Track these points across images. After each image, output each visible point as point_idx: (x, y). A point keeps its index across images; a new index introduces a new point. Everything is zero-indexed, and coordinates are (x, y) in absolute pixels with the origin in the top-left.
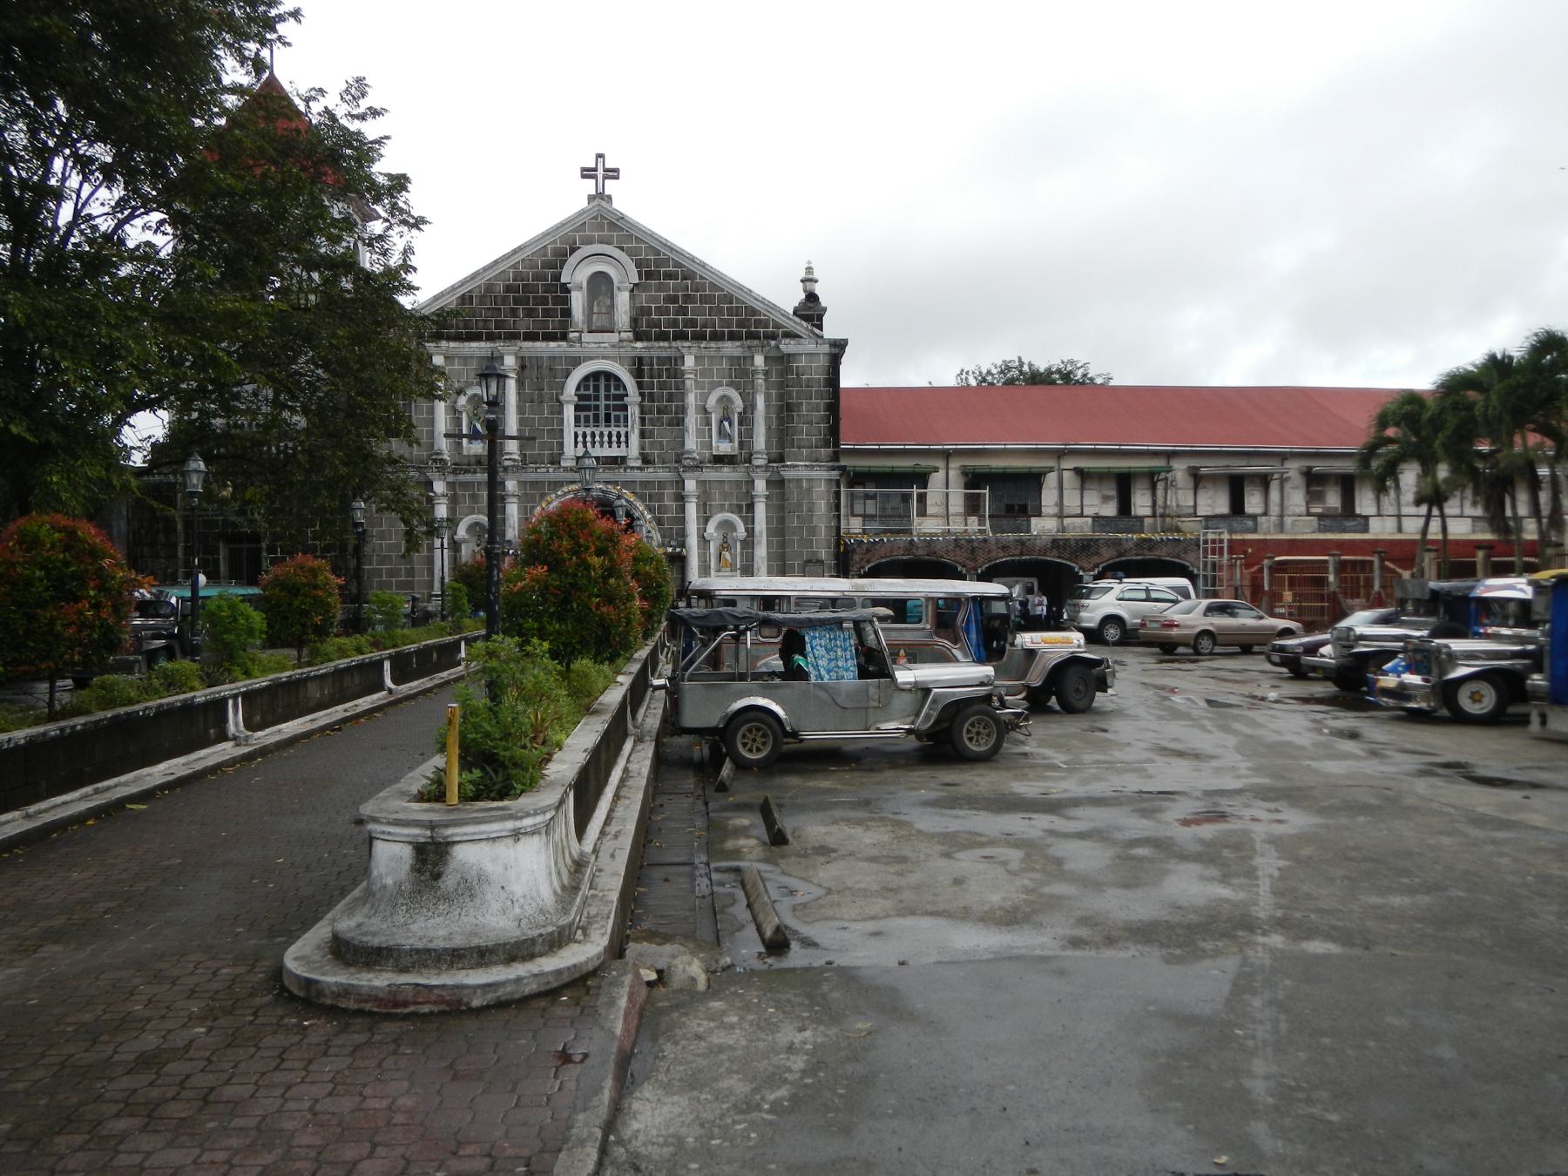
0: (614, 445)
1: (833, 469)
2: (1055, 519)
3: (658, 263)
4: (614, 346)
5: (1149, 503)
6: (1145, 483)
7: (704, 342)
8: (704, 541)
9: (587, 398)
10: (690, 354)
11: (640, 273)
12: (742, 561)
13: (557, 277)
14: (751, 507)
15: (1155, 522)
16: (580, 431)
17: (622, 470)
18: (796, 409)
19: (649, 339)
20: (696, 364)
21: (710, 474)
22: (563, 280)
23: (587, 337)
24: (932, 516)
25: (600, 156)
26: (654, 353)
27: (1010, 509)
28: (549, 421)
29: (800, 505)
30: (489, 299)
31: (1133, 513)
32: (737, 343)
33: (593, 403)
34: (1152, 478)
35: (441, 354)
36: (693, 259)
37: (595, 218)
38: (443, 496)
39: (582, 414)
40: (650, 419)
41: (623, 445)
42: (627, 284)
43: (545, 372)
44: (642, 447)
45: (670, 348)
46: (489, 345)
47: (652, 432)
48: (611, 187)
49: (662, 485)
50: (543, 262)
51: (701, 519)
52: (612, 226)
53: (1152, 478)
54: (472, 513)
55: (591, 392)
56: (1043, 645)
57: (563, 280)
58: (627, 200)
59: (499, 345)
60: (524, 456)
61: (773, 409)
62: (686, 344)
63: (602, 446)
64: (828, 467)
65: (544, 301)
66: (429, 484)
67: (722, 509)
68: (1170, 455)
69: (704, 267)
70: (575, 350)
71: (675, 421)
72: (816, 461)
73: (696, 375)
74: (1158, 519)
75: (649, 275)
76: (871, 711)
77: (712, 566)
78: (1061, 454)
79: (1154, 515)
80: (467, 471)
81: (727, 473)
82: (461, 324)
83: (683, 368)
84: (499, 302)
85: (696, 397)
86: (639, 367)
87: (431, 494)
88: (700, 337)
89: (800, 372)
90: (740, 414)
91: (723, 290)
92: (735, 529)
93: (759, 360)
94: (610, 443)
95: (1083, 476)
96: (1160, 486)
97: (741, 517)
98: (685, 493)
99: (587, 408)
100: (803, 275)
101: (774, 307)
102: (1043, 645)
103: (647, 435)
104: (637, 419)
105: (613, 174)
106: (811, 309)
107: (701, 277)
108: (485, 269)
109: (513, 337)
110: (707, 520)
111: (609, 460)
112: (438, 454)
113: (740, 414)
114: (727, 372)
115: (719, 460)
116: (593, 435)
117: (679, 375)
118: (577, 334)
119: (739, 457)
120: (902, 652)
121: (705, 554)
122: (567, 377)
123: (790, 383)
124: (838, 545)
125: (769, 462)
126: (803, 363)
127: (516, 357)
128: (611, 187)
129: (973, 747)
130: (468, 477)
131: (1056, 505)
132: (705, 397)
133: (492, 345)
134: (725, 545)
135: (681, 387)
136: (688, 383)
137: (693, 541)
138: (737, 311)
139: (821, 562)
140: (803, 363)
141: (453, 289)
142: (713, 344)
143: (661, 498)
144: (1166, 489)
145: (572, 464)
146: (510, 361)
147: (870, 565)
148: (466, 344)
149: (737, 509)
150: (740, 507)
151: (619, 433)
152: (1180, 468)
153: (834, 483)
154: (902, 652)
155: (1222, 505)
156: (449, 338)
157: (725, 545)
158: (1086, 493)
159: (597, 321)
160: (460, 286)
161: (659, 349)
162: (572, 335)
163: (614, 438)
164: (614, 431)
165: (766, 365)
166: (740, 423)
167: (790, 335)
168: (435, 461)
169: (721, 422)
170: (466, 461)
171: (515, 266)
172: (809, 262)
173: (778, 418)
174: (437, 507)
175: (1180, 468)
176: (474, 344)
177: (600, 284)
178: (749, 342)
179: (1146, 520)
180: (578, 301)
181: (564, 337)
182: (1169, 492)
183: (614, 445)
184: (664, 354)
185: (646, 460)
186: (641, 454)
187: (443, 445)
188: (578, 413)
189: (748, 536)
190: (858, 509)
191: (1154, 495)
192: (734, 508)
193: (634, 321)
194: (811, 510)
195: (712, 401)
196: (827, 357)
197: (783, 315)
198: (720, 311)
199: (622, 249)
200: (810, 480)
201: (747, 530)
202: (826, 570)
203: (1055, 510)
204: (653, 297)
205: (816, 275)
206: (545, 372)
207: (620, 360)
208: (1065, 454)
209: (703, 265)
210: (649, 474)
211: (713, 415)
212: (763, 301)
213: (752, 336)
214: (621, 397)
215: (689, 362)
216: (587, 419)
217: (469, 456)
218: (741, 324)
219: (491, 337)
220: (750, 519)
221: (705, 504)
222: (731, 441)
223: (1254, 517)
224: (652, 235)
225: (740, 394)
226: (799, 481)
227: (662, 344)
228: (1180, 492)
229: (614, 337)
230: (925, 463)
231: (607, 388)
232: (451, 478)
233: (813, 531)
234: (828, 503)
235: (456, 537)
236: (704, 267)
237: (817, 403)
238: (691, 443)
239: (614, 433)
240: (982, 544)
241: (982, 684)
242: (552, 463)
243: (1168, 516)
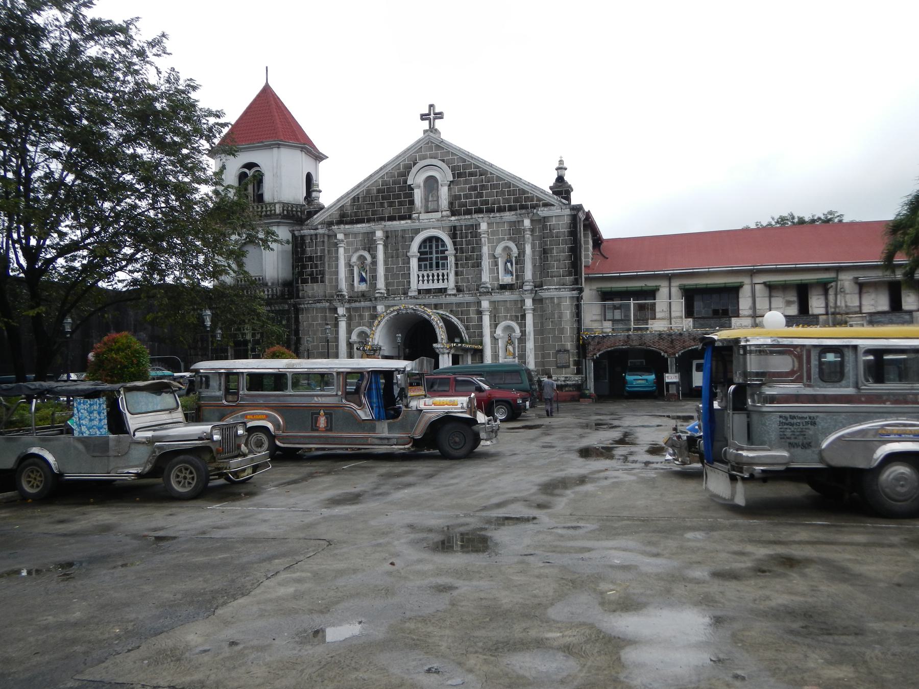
0: (441, 281)
1: (573, 290)
2: (750, 318)
3: (465, 167)
4: (438, 220)
5: (823, 305)
6: (820, 290)
7: (492, 214)
8: (495, 340)
9: (426, 253)
10: (484, 221)
11: (454, 175)
12: (518, 352)
13: (405, 182)
14: (524, 317)
15: (828, 319)
16: (420, 273)
17: (444, 296)
18: (550, 252)
19: (460, 214)
20: (488, 228)
21: (497, 297)
22: (409, 183)
23: (423, 216)
24: (659, 319)
25: (431, 106)
26: (463, 223)
27: (716, 313)
28: (402, 269)
29: (553, 314)
30: (368, 198)
31: (810, 312)
32: (513, 213)
33: (429, 256)
34: (824, 287)
35: (342, 233)
36: (485, 162)
37: (428, 143)
38: (343, 316)
39: (423, 263)
40: (461, 264)
41: (446, 281)
43: (400, 239)
44: (457, 282)
45: (472, 219)
46: (367, 225)
47: (462, 272)
48: (438, 124)
49: (468, 304)
50: (398, 173)
51: (493, 326)
52: (438, 147)
53: (824, 287)
55: (428, 249)
56: (433, 406)
57: (409, 183)
58: (448, 132)
59: (372, 224)
60: (388, 290)
61: (537, 253)
62: (481, 216)
63: (433, 282)
64: (570, 288)
65: (399, 197)
66: (335, 310)
67: (506, 318)
68: (839, 270)
69: (491, 166)
70: (416, 225)
71: (476, 265)
72: (563, 285)
73: (488, 235)
74: (830, 316)
75: (460, 175)
76: (111, 459)
77: (500, 354)
78: (752, 273)
79: (827, 314)
80: (356, 301)
81: (507, 296)
82: (353, 215)
83: (479, 231)
84: (374, 199)
85: (489, 249)
86: (454, 232)
87: (336, 315)
88: (491, 210)
89: (552, 228)
90: (516, 257)
91: (505, 180)
92: (513, 330)
93: (527, 223)
94: (438, 280)
95: (771, 288)
96: (831, 292)
97: (518, 323)
98: (481, 309)
99: (426, 260)
100: (557, 165)
101: (536, 188)
102: (433, 406)
103: (459, 273)
104: (453, 265)
105: (440, 115)
106: (562, 189)
107: (491, 173)
108: (365, 181)
109: (382, 219)
110: (496, 326)
111: (437, 291)
112: (340, 292)
113: (516, 257)
114: (507, 231)
115: (503, 287)
116: (428, 276)
117: (478, 236)
118: (417, 215)
119: (516, 285)
120: (322, 412)
121: (495, 347)
122: (412, 242)
123: (545, 236)
124: (578, 340)
125: (535, 287)
126: (554, 222)
127: (384, 232)
128: (438, 124)
129: (179, 489)
130: (357, 305)
131: (750, 308)
132: (494, 248)
133: (369, 225)
134: (509, 342)
135: (479, 243)
136: (483, 240)
137: (487, 340)
138: (514, 192)
139: (567, 351)
140: (554, 222)
141: (348, 194)
142: (498, 215)
143: (468, 313)
144: (836, 295)
145: (416, 293)
146: (379, 234)
147: (600, 353)
148: (355, 226)
149: (515, 318)
150: (517, 317)
151: (443, 273)
152: (846, 279)
153: (575, 299)
154: (322, 412)
155: (882, 303)
156: (347, 223)
157: (510, 341)
158: (773, 299)
159: (431, 206)
160: (351, 192)
161: (464, 221)
162: (414, 216)
163: (441, 277)
164: (436, 273)
165: (532, 225)
166: (516, 264)
167: (547, 205)
168: (338, 296)
169: (506, 263)
170: (356, 295)
171: (382, 177)
172: (561, 157)
173: (540, 258)
174: (340, 322)
175: (846, 279)
176: (359, 226)
177: (431, 183)
178: (519, 212)
179: (821, 317)
180: (418, 195)
181: (410, 218)
182: (839, 296)
183: (441, 281)
184: (469, 223)
185: (459, 290)
186: (456, 286)
187: (343, 286)
188: (420, 263)
189: (522, 336)
190: (609, 316)
191: (827, 299)
192: (513, 318)
193: (451, 204)
194: (560, 317)
195: (499, 250)
196: (569, 217)
197: (542, 192)
198: (503, 193)
199: (443, 161)
200: (559, 298)
201: (521, 331)
202: (571, 356)
203: (750, 312)
204: (462, 188)
205: (565, 165)
206: (400, 239)
207: (442, 228)
208: (754, 273)
209: (491, 165)
210: (460, 298)
211: (500, 259)
212: (529, 184)
213: (523, 207)
214: (443, 252)
215: (484, 226)
216: (425, 265)
217: (358, 292)
218: (516, 200)
219: (369, 221)
220: (523, 324)
221: (495, 316)
222: (512, 275)
223: (910, 312)
224: (460, 150)
225: (516, 245)
226: (552, 298)
227: (466, 217)
228: (848, 296)
229: (438, 215)
230: (651, 284)
231: (437, 247)
232: (347, 305)
233: (562, 331)
234: (571, 312)
235: (350, 340)
236: (491, 166)
237: (564, 248)
238: (486, 277)
239: (441, 274)
240: (678, 337)
241: (200, 439)
242: (404, 294)
243: (839, 314)
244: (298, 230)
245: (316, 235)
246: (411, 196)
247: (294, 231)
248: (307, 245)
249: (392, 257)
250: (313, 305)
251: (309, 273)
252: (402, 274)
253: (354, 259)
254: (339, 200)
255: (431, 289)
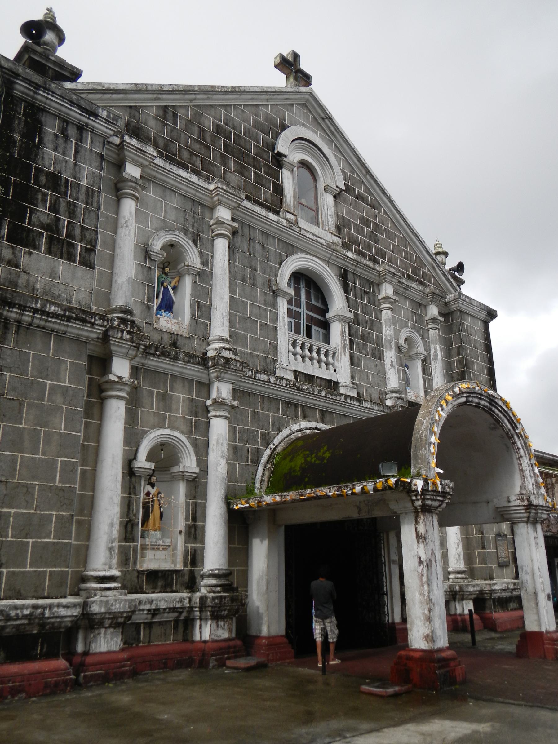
10: (391, 283)
35: (141, 166)
42: (335, 187)
54: (161, 425)
84: (208, 139)
90: (422, 360)
103: (356, 360)
107: (385, 213)
117: (377, 303)
218: (415, 270)
231: (308, 297)
244: (31, 83)
245: (81, 128)
246: (278, 177)
247: (17, 75)
248: (48, 139)
249: (243, 280)
250: (55, 324)
251: (45, 220)
252: (262, 325)
253: (157, 245)
254: (138, 89)
255: (314, 376)
